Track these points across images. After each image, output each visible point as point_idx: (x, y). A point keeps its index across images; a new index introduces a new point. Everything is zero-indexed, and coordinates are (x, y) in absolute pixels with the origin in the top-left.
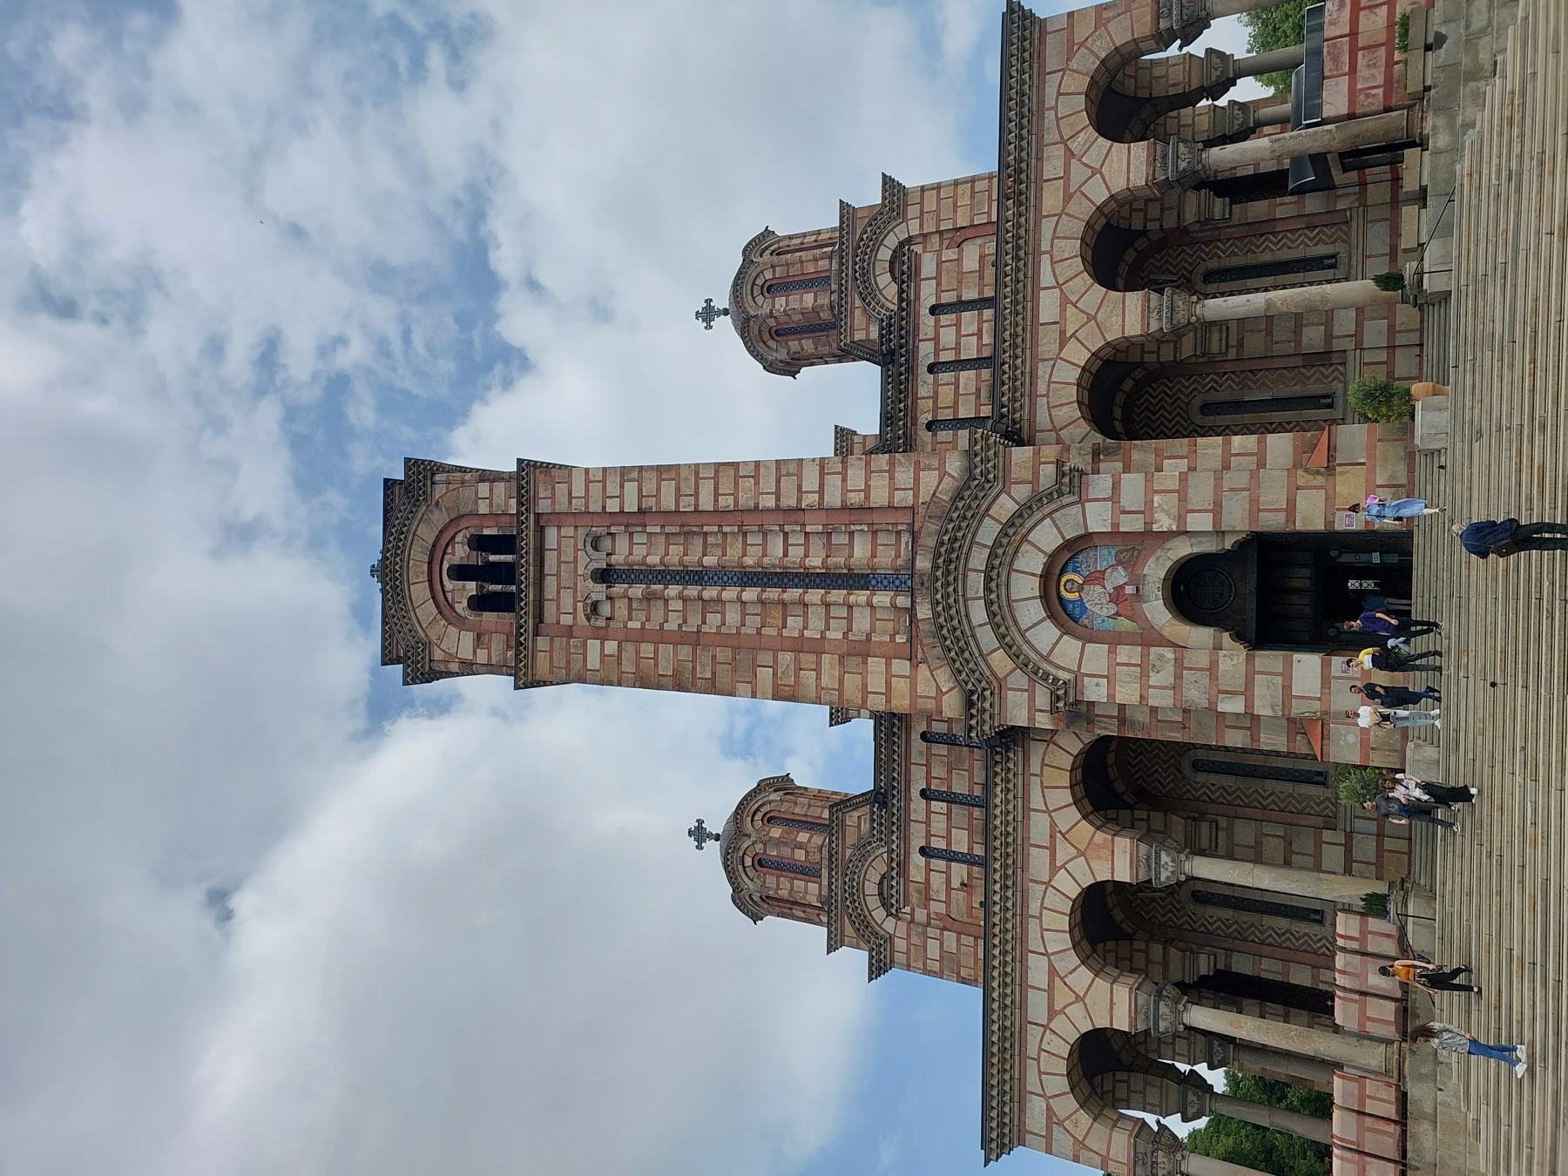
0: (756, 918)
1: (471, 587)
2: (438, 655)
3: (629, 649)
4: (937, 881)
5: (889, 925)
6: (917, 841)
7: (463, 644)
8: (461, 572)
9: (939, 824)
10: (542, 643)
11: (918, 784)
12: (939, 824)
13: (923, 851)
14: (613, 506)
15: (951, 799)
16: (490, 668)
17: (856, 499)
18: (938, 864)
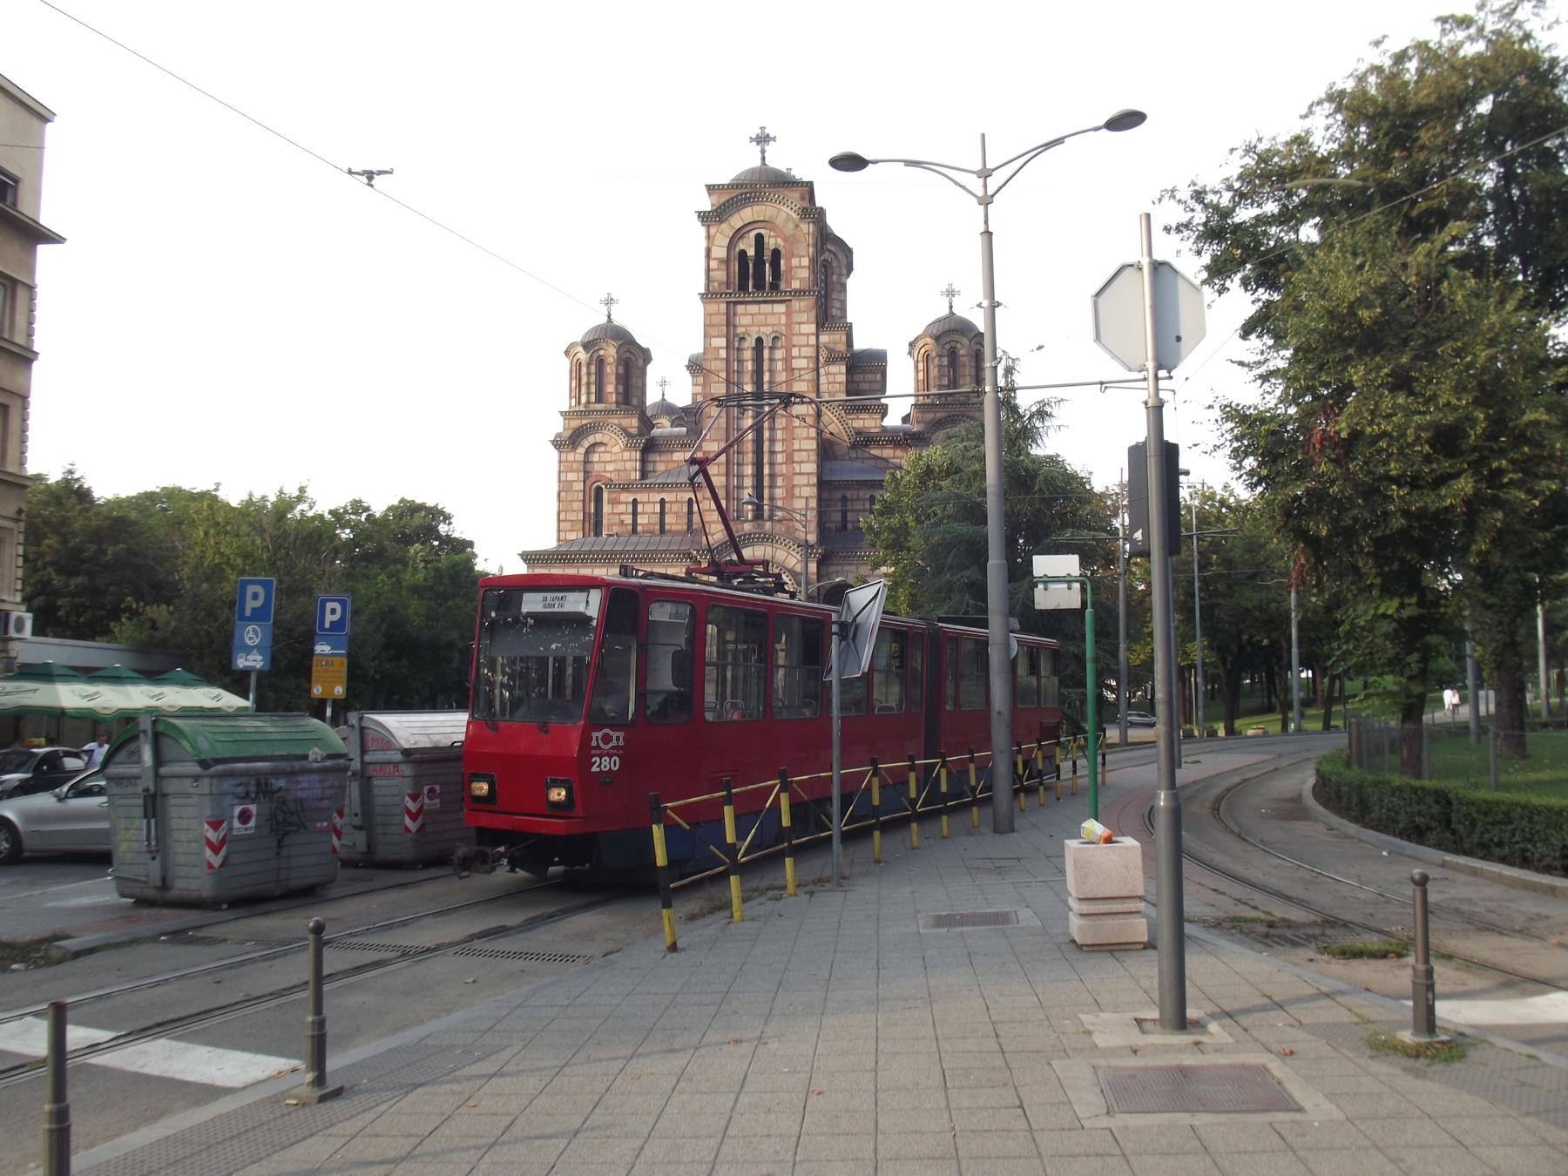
0: (567, 353)
1: (751, 252)
2: (713, 230)
3: (723, 365)
4: (622, 508)
5: (581, 450)
6: (639, 497)
7: (720, 252)
8: (759, 239)
9: (649, 508)
10: (723, 307)
11: (667, 497)
12: (649, 508)
13: (635, 501)
14: (795, 352)
15: (662, 513)
16: (708, 270)
17: (797, 491)
18: (630, 509)
